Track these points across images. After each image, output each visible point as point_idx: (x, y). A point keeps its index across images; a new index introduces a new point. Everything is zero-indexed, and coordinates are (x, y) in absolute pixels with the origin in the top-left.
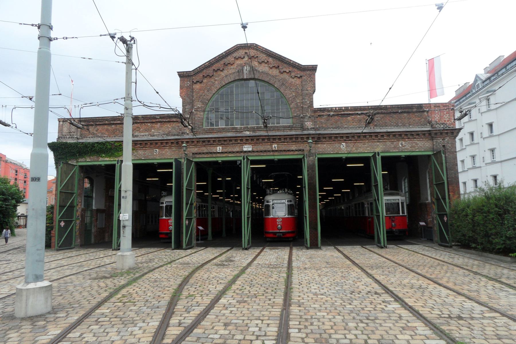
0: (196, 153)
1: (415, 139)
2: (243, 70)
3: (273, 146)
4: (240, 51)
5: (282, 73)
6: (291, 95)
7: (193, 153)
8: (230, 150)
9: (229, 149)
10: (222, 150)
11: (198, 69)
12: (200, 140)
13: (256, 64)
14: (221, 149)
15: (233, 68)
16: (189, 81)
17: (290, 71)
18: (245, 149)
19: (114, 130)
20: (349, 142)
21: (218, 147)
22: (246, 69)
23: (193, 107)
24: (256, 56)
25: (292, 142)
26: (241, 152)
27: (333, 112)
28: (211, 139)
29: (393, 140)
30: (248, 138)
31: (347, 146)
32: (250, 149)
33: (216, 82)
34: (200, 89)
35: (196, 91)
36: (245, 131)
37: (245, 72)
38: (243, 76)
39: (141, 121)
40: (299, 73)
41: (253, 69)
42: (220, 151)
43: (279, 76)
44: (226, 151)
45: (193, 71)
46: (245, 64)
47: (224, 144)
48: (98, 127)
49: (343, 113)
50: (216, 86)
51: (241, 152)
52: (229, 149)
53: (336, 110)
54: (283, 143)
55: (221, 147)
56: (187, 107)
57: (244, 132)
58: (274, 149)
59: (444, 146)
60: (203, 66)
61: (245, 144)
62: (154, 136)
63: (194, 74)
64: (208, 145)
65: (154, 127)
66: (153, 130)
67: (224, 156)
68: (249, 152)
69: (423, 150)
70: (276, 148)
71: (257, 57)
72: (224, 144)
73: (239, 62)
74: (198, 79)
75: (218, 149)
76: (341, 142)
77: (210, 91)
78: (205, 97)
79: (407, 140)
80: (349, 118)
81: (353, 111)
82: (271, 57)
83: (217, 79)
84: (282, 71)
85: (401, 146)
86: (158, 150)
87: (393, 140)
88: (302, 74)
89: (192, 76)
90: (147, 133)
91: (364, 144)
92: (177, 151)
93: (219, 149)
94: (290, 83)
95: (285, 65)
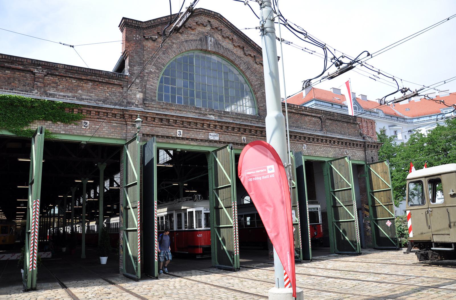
0: (148, 135)
1: (354, 149)
3: (242, 138)
4: (202, 17)
5: (247, 56)
7: (143, 134)
8: (193, 136)
9: (192, 135)
10: (183, 135)
11: (152, 22)
12: (157, 117)
13: (220, 38)
14: (181, 133)
15: (194, 35)
16: (139, 34)
17: (254, 56)
18: (211, 138)
19: (9, 78)
20: (310, 144)
21: (178, 130)
23: (144, 69)
24: (219, 28)
25: (261, 136)
26: (206, 141)
27: (295, 110)
28: (171, 118)
29: (340, 147)
30: (217, 124)
31: (308, 148)
32: (217, 138)
33: (174, 45)
34: (153, 49)
35: (147, 49)
36: (210, 115)
38: (207, 47)
39: (62, 74)
42: (181, 136)
43: (243, 58)
44: (187, 137)
45: (145, 22)
46: (207, 33)
47: (187, 127)
49: (302, 112)
50: (173, 49)
51: (206, 141)
52: (192, 135)
53: (297, 108)
54: (252, 136)
55: (181, 131)
56: (135, 68)
57: (209, 116)
58: (243, 142)
60: (159, 20)
61: (212, 130)
62: (82, 99)
63: (146, 28)
64: (166, 125)
65: (83, 87)
66: (80, 92)
67: (184, 143)
68: (216, 141)
69: (359, 159)
70: (245, 141)
71: (221, 29)
72: (187, 127)
73: (200, 29)
75: (178, 133)
76: (303, 143)
77: (166, 55)
78: (159, 60)
79: (349, 148)
80: (307, 119)
81: (310, 112)
82: (236, 34)
83: (175, 41)
85: (345, 154)
86: (88, 122)
87: (340, 147)
89: (144, 29)
90: (70, 94)
91: (320, 148)
92: (119, 128)
93: (179, 133)
94: (255, 69)
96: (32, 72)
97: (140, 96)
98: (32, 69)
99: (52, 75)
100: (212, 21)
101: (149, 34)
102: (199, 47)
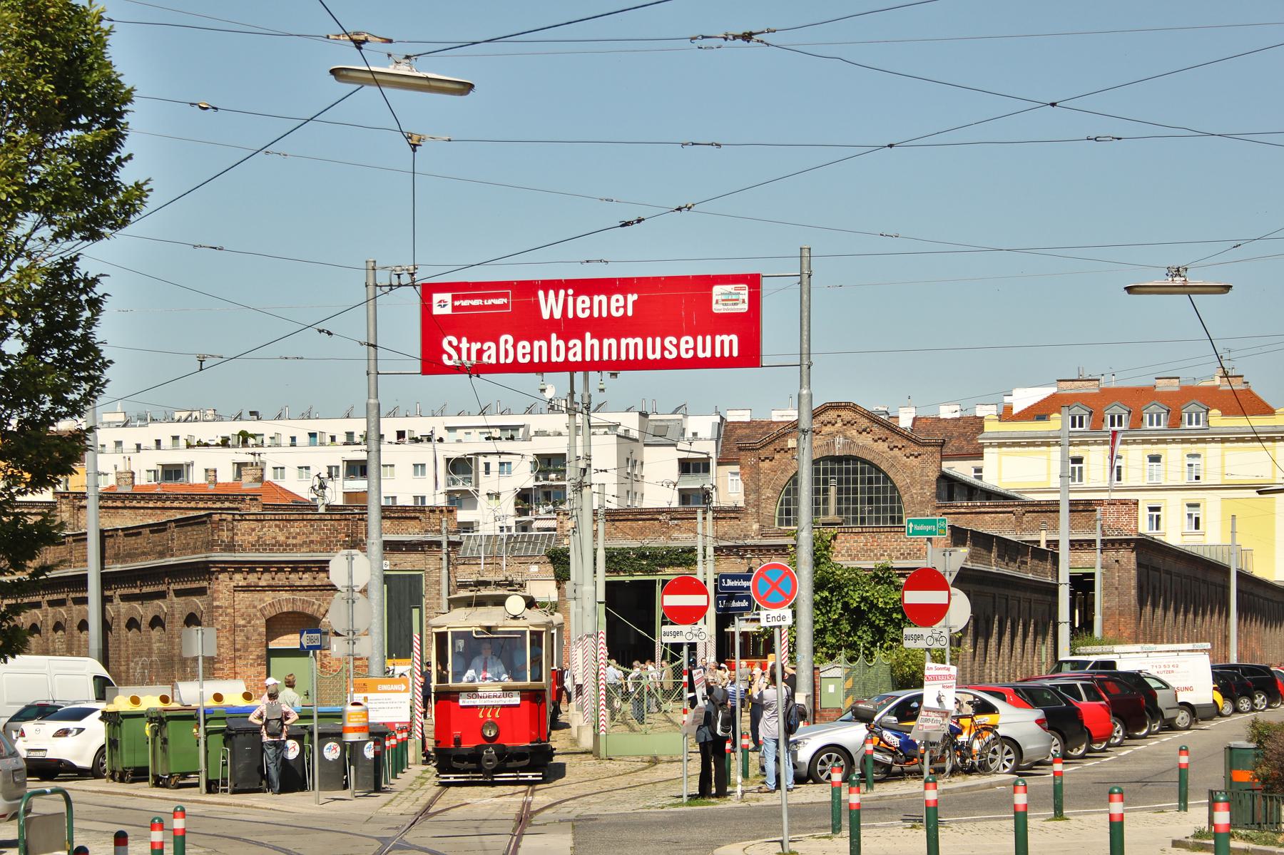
2: (834, 442)
6: (905, 482)
22: (840, 440)
24: (853, 422)
37: (837, 446)
40: (917, 450)
41: (850, 443)
48: (617, 523)
56: (751, 497)
59: (1117, 561)
73: (829, 429)
74: (767, 454)
80: (987, 517)
84: (892, 445)
88: (921, 450)
89: (759, 449)
95: (897, 437)
96: (658, 519)
97: (756, 526)
98: (658, 516)
99: (675, 519)
100: (843, 413)
101: (764, 453)
102: (825, 454)
